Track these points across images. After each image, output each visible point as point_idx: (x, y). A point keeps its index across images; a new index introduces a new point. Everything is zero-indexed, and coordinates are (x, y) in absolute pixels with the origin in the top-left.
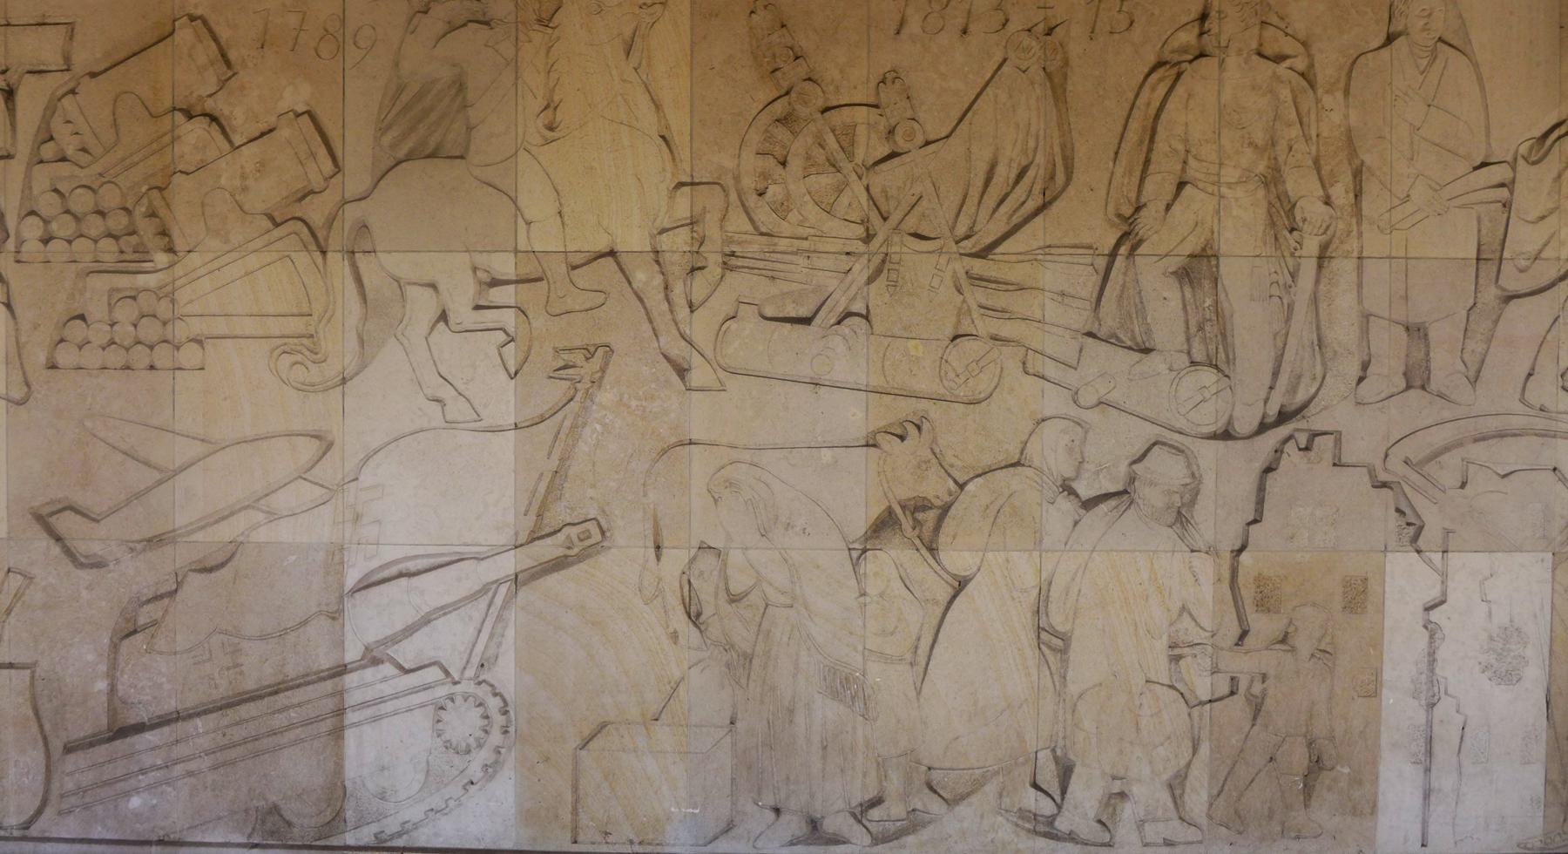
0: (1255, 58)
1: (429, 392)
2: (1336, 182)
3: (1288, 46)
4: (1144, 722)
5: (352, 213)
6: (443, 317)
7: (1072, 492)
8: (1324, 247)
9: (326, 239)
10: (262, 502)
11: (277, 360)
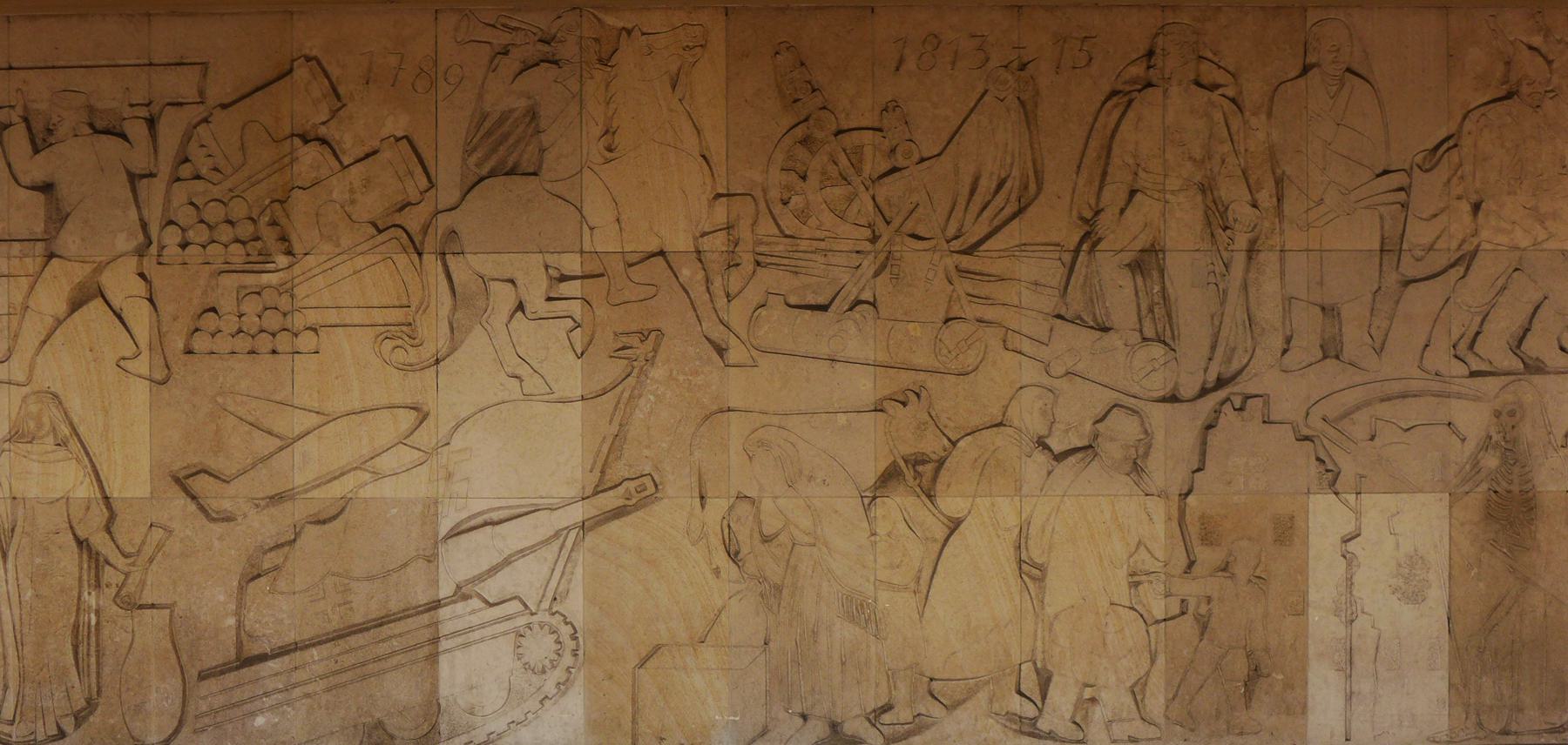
0: (1194, 87)
1: (509, 370)
2: (1263, 188)
3: (1219, 77)
4: (1110, 637)
5: (444, 221)
6: (520, 307)
7: (1046, 447)
8: (1253, 242)
9: (422, 243)
11: (381, 344)
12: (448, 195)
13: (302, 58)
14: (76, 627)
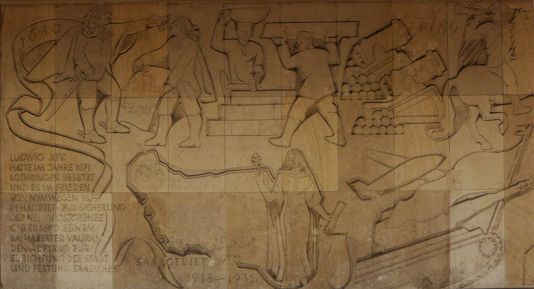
1: (477, 140)
5: (451, 83)
10: (423, 177)
11: (428, 130)
12: (452, 72)
13: (396, 20)
14: (308, 243)
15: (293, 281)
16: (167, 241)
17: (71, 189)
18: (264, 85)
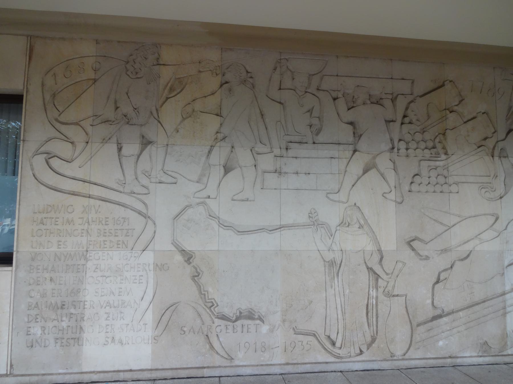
5: (501, 145)
11: (481, 190)
14: (367, 305)
15: (352, 348)
16: (216, 305)
17: (105, 246)
18: (320, 138)
